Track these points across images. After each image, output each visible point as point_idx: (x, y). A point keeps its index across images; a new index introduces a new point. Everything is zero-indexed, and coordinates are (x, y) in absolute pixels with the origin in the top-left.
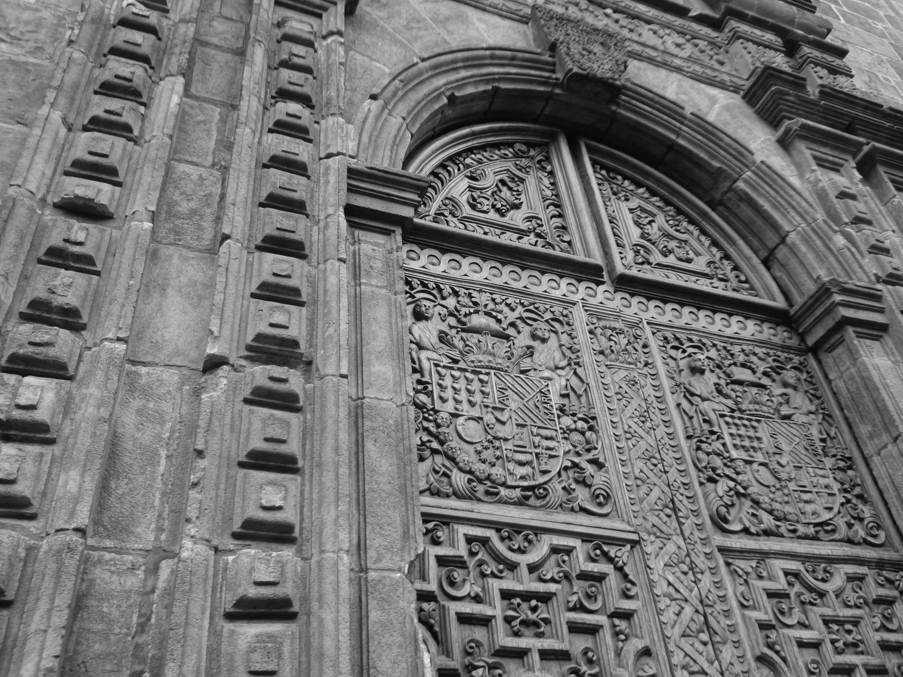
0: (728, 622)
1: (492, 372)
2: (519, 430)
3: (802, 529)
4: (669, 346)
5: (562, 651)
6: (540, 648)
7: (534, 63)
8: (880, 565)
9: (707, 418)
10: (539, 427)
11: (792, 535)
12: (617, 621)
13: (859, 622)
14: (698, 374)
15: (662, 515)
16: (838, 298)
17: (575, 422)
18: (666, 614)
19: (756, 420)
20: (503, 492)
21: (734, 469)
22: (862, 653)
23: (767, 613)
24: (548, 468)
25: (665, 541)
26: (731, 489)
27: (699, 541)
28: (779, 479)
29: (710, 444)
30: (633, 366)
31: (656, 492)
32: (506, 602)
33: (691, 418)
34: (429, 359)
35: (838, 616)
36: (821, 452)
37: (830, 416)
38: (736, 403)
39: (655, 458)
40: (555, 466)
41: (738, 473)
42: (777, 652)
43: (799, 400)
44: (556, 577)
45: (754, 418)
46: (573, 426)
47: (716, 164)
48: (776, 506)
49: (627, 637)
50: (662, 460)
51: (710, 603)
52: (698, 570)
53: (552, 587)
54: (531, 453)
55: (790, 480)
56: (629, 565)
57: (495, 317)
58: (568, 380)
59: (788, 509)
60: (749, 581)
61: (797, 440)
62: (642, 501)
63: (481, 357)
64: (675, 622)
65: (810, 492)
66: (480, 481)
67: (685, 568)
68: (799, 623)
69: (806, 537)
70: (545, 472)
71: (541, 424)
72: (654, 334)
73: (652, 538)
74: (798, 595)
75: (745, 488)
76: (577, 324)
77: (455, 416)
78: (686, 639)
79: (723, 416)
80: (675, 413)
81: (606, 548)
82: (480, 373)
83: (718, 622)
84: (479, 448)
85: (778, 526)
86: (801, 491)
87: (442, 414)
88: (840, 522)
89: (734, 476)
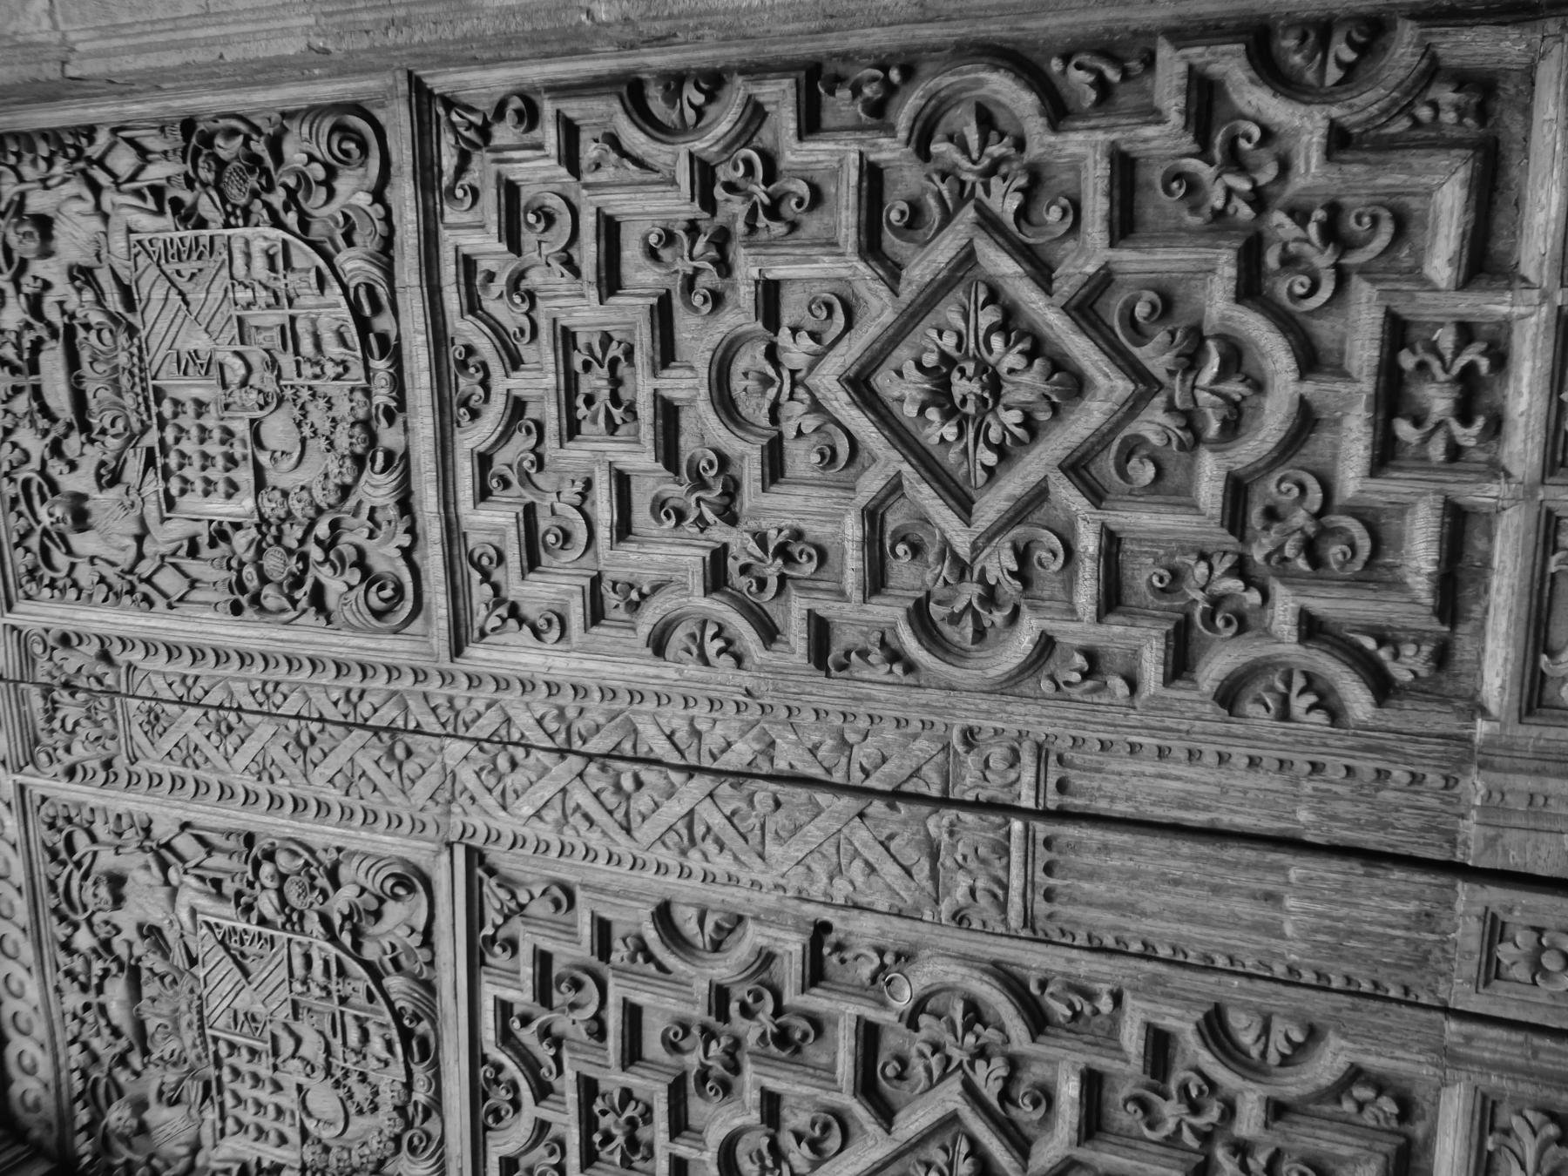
0: (597, 695)
1: (208, 1032)
2: (303, 1014)
3: (382, 397)
4: (48, 574)
5: (669, 1098)
6: (667, 1136)
9: (186, 544)
10: (291, 974)
11: (399, 419)
12: (615, 957)
13: (565, 329)
14: (90, 521)
15: (410, 768)
17: (263, 888)
18: (592, 844)
19: (158, 403)
20: (421, 1095)
21: (283, 520)
22: (629, 353)
23: (571, 594)
24: (361, 987)
25: (458, 788)
26: (327, 559)
27: (447, 691)
28: (281, 401)
29: (242, 564)
30: (117, 700)
31: (365, 762)
32: (603, 1155)
33: (193, 584)
34: (215, 1146)
35: (558, 390)
36: (189, 234)
37: (90, 132)
38: (132, 439)
39: (298, 733)
41: (289, 513)
42: (643, 596)
44: (552, 1052)
45: (154, 410)
46: (273, 896)
48: (342, 441)
49: (642, 947)
50: (298, 717)
51: (563, 735)
52: (503, 732)
53: (570, 1074)
54: (342, 1013)
55: (273, 365)
56: (517, 875)
57: (103, 978)
58: (186, 872)
59: (342, 408)
60: (511, 599)
61: (173, 294)
62: (388, 803)
63: (188, 1043)
64: (604, 833)
65: (293, 319)
66: (409, 1125)
67: (503, 763)
68: (579, 509)
69: (398, 383)
70: (371, 997)
71: (285, 974)
72: (29, 597)
73: (456, 809)
74: (526, 479)
75: (320, 511)
76: (65, 795)
77: (304, 1134)
78: (634, 825)
79: (170, 503)
81: (488, 931)
82: (216, 1053)
83: (598, 728)
84: (352, 1110)
85: (389, 455)
86: (297, 352)
87: (308, 1158)
89: (298, 532)
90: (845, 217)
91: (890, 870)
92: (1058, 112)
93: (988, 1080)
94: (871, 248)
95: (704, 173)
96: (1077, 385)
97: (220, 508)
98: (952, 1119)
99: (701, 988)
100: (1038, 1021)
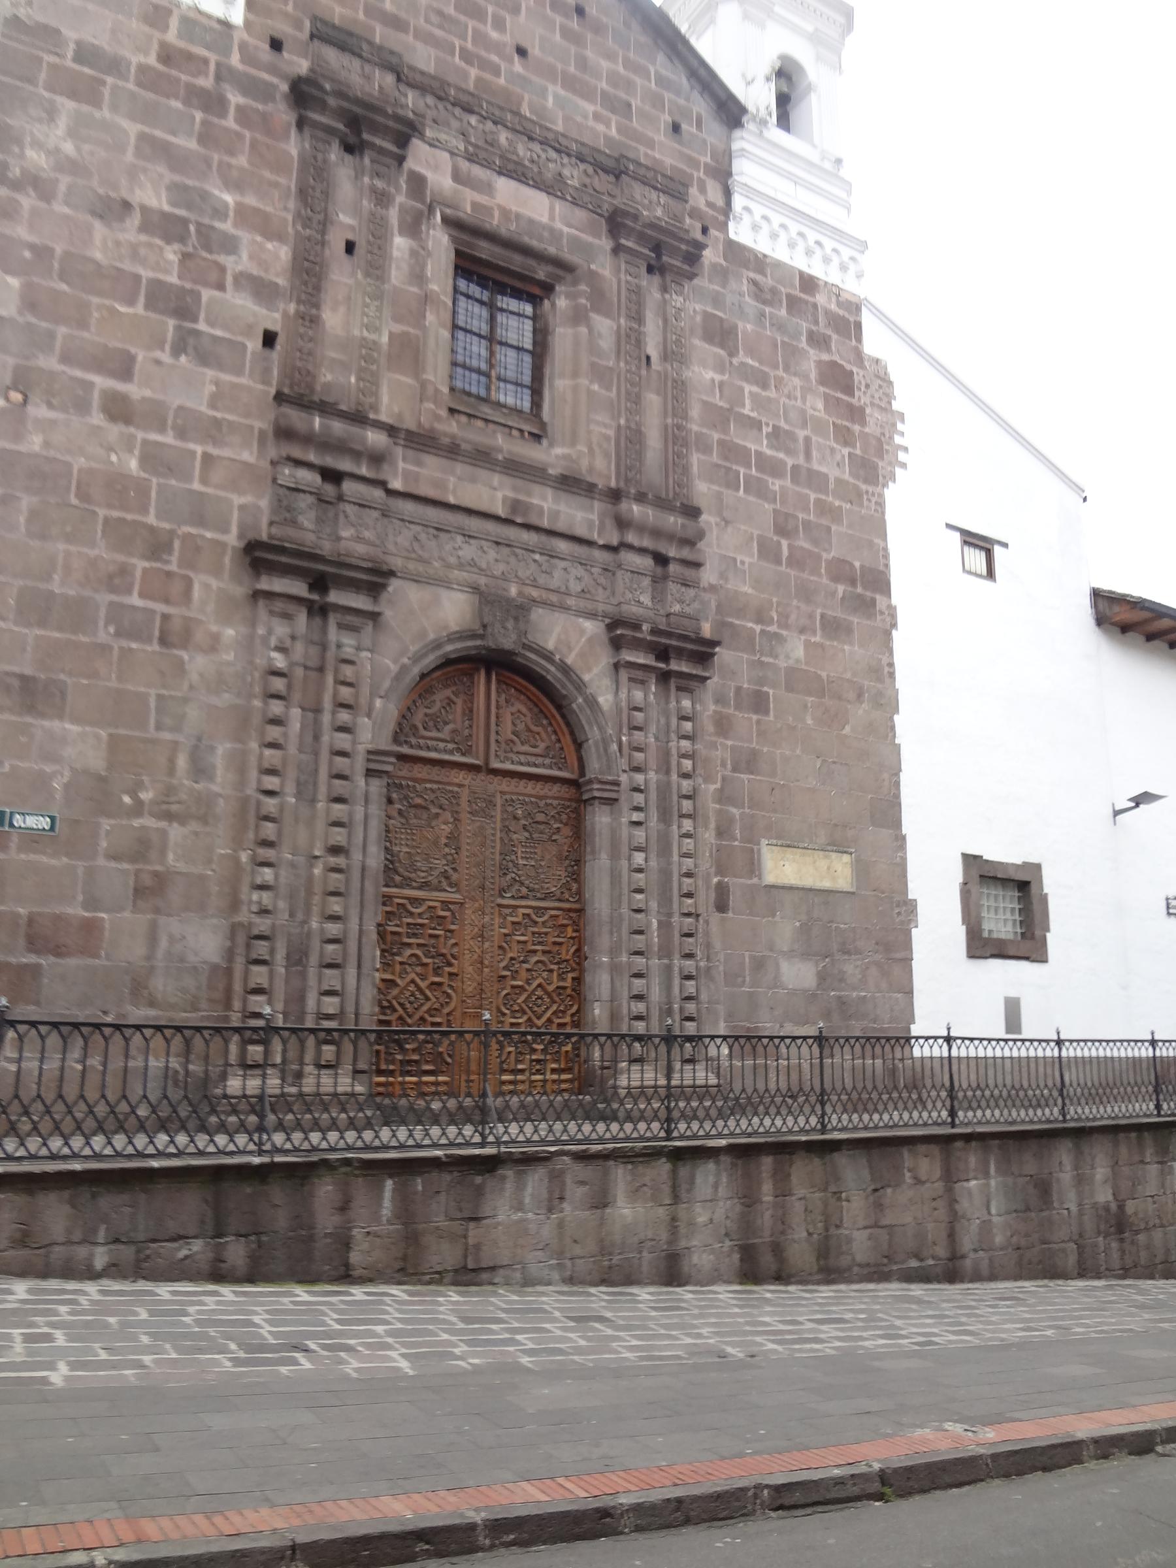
3: (539, 895)
7: (474, 636)
8: (570, 910)
16: (596, 786)
20: (414, 884)
40: (436, 873)
43: (567, 831)
47: (564, 692)
80: (498, 841)
88: (558, 893)
90: (561, 984)
91: (470, 989)
92: (573, 1015)
93: (437, 1006)
94: (558, 987)
95: (567, 961)
96: (539, 1018)
97: (519, 854)
98: (427, 999)
99: (444, 951)
100: (448, 1014)
